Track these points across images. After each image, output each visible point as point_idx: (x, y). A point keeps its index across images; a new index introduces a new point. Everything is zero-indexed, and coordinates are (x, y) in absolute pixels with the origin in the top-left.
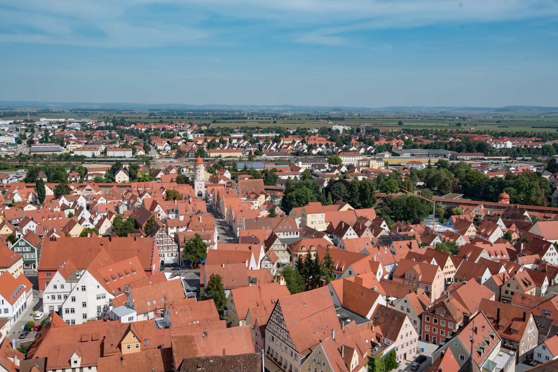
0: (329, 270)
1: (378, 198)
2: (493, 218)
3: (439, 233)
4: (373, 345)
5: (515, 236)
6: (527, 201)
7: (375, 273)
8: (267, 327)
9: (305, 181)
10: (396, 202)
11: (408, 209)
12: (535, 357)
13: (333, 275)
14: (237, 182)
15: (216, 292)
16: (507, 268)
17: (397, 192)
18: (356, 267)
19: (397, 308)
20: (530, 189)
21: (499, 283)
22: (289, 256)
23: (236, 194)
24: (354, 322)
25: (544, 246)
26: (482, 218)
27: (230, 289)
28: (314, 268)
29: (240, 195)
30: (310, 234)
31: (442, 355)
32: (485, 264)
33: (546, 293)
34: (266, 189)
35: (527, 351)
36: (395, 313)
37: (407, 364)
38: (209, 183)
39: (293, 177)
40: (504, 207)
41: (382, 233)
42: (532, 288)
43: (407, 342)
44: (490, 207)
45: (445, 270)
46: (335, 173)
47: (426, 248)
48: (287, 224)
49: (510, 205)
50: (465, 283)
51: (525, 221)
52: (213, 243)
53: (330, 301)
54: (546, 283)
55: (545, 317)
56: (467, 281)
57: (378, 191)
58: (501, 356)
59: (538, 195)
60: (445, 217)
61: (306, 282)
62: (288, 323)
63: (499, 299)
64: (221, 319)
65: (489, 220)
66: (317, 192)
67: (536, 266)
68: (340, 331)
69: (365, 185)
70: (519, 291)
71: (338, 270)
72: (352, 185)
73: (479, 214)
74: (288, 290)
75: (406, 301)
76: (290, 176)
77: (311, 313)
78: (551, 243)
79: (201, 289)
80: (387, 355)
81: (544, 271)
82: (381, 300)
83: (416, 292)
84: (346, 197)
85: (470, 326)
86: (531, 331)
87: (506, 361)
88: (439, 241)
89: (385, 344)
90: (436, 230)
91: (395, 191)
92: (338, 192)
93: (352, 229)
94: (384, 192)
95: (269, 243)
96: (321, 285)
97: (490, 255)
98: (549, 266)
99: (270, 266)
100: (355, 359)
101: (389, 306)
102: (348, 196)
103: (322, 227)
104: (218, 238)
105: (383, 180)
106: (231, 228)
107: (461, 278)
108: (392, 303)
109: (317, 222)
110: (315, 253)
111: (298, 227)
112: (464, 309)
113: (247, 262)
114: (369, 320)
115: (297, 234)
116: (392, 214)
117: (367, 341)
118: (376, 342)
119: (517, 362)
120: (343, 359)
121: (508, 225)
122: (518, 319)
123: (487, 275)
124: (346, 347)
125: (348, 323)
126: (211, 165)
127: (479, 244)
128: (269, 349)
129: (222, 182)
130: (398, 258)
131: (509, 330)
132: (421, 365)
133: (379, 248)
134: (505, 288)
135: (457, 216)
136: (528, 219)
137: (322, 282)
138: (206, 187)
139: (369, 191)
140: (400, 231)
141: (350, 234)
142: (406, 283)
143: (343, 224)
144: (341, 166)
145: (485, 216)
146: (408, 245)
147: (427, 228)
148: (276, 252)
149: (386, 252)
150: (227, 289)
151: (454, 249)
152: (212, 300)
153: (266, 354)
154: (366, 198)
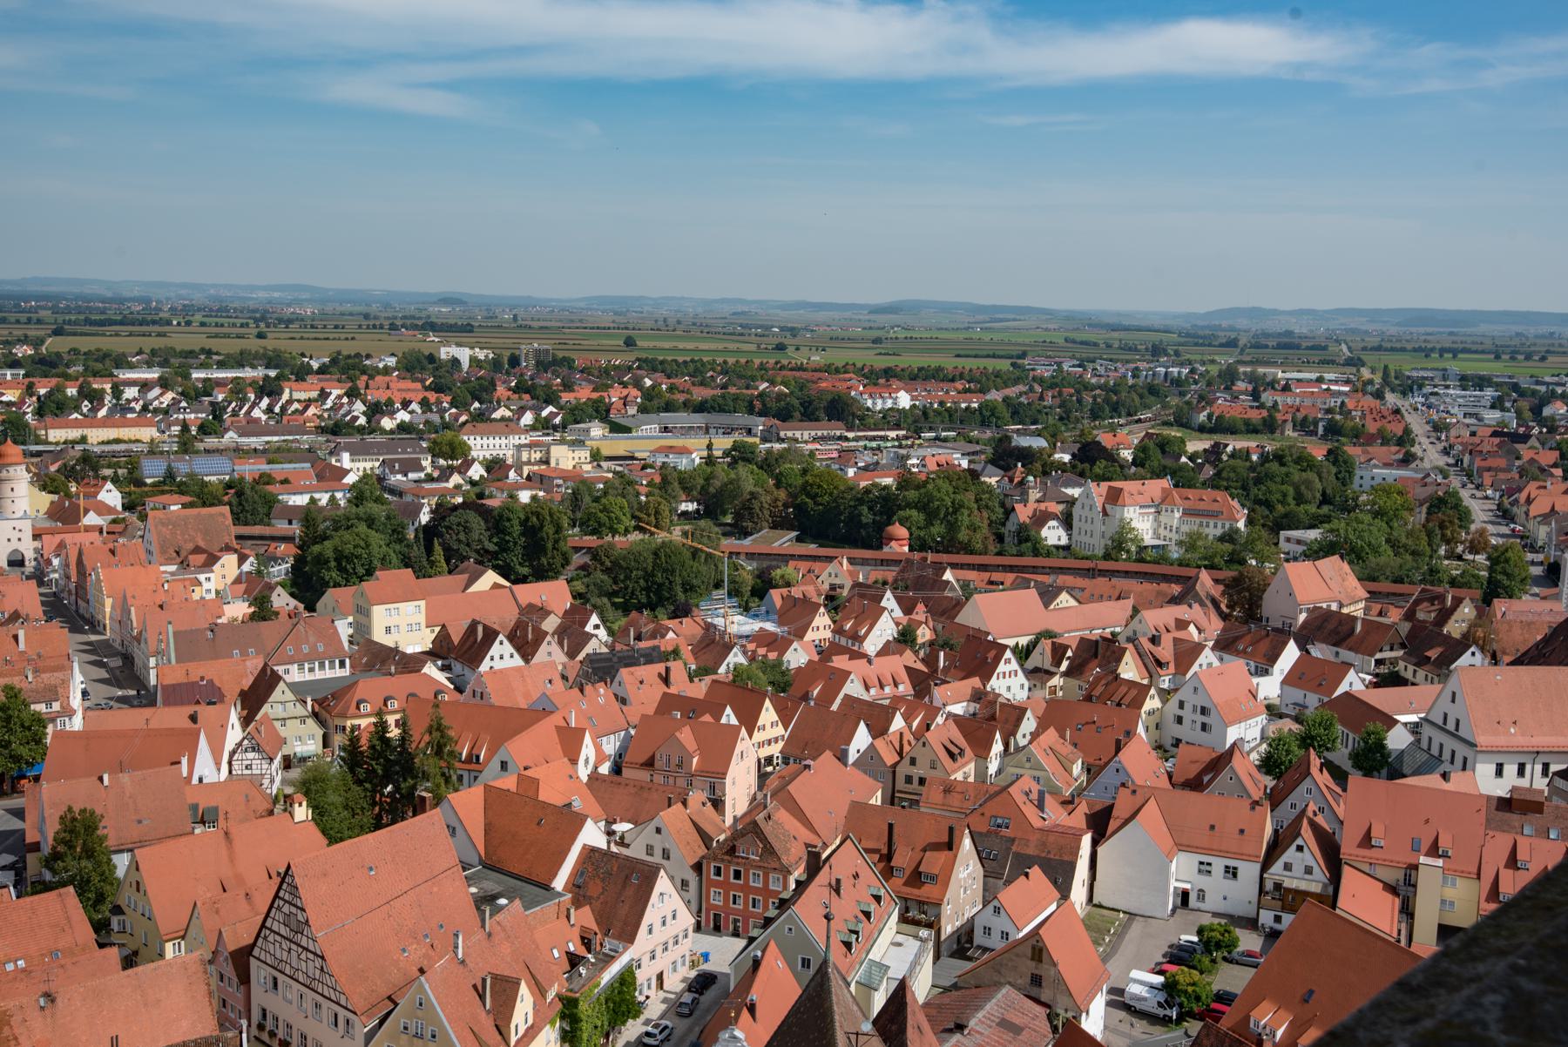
0: (443, 764)
1: (577, 549)
2: (872, 592)
3: (741, 637)
4: (574, 961)
5: (924, 634)
6: (950, 544)
7: (574, 761)
8: (256, 952)
9: (361, 510)
10: (624, 558)
11: (659, 578)
12: (979, 938)
13: (454, 778)
14: (143, 517)
15: (84, 863)
16: (908, 719)
17: (627, 531)
18: (520, 749)
19: (636, 851)
20: (955, 512)
21: (890, 758)
22: (319, 732)
23: (143, 555)
24: (517, 902)
25: (991, 655)
26: (845, 593)
27: (131, 850)
28: (396, 763)
29: (154, 558)
30: (383, 662)
31: (756, 964)
32: (858, 710)
33: (999, 772)
34: (239, 537)
35: (958, 924)
36: (632, 865)
37: (665, 1001)
38: (48, 524)
39: (324, 499)
40: (897, 562)
42: (967, 763)
43: (663, 940)
44: (864, 562)
45: (758, 736)
46: (451, 484)
47: (708, 679)
48: (312, 639)
49: (911, 556)
50: (807, 767)
51: (948, 593)
52: (70, 713)
53: (446, 853)
54: (998, 747)
55: (997, 833)
56: (814, 759)
57: (577, 530)
58: (900, 945)
59: (974, 528)
60: (753, 595)
61: (374, 804)
62: (321, 933)
63: (891, 799)
64: (101, 946)
65: (862, 596)
66: (400, 541)
67: (974, 707)
68: (479, 936)
69: (538, 515)
70: (938, 773)
71: (469, 760)
72: (501, 516)
73: (837, 581)
74: (320, 835)
75: (658, 831)
76: (317, 496)
77: (392, 893)
78: (1006, 647)
79: (32, 859)
80: (611, 985)
81: (993, 718)
82: (592, 835)
83: (685, 803)
84: (487, 551)
85: (823, 877)
86: (967, 870)
87: (911, 958)
88: (741, 660)
89: (606, 955)
90: (733, 629)
91: (621, 528)
92: (462, 536)
93: (506, 642)
94: (592, 533)
95: (254, 698)
96: (419, 807)
97: (867, 688)
98: (1002, 705)
99: (259, 766)
100: (524, 1008)
101: (614, 849)
102: (492, 547)
103: (417, 641)
104: (85, 693)
105: (587, 499)
106: (128, 659)
107: (798, 753)
108: (622, 838)
109: (404, 628)
110: (398, 716)
111: (346, 645)
112: (805, 835)
113: (185, 761)
114: (560, 895)
115: (342, 664)
116: (615, 594)
117: (555, 952)
118: (582, 951)
119: (937, 957)
120: (488, 1012)
121: (908, 609)
122: (936, 847)
123: (861, 739)
124: (495, 977)
125: (502, 908)
126: (53, 468)
127: (840, 662)
128: (264, 1016)
129: (92, 519)
130: (634, 712)
131: (916, 878)
132: (702, 999)
133: (582, 691)
134: (902, 771)
135: (784, 591)
136: (953, 589)
137: (423, 799)
138: (36, 537)
139: (551, 532)
140: (638, 638)
141: (502, 656)
142: (659, 779)
143: (480, 629)
144: (468, 464)
145: (853, 587)
146: (660, 675)
147: (709, 627)
148: (277, 724)
149: (601, 700)
150: (121, 851)
151: (778, 677)
152: (71, 889)
153: (254, 1031)
154: (543, 550)
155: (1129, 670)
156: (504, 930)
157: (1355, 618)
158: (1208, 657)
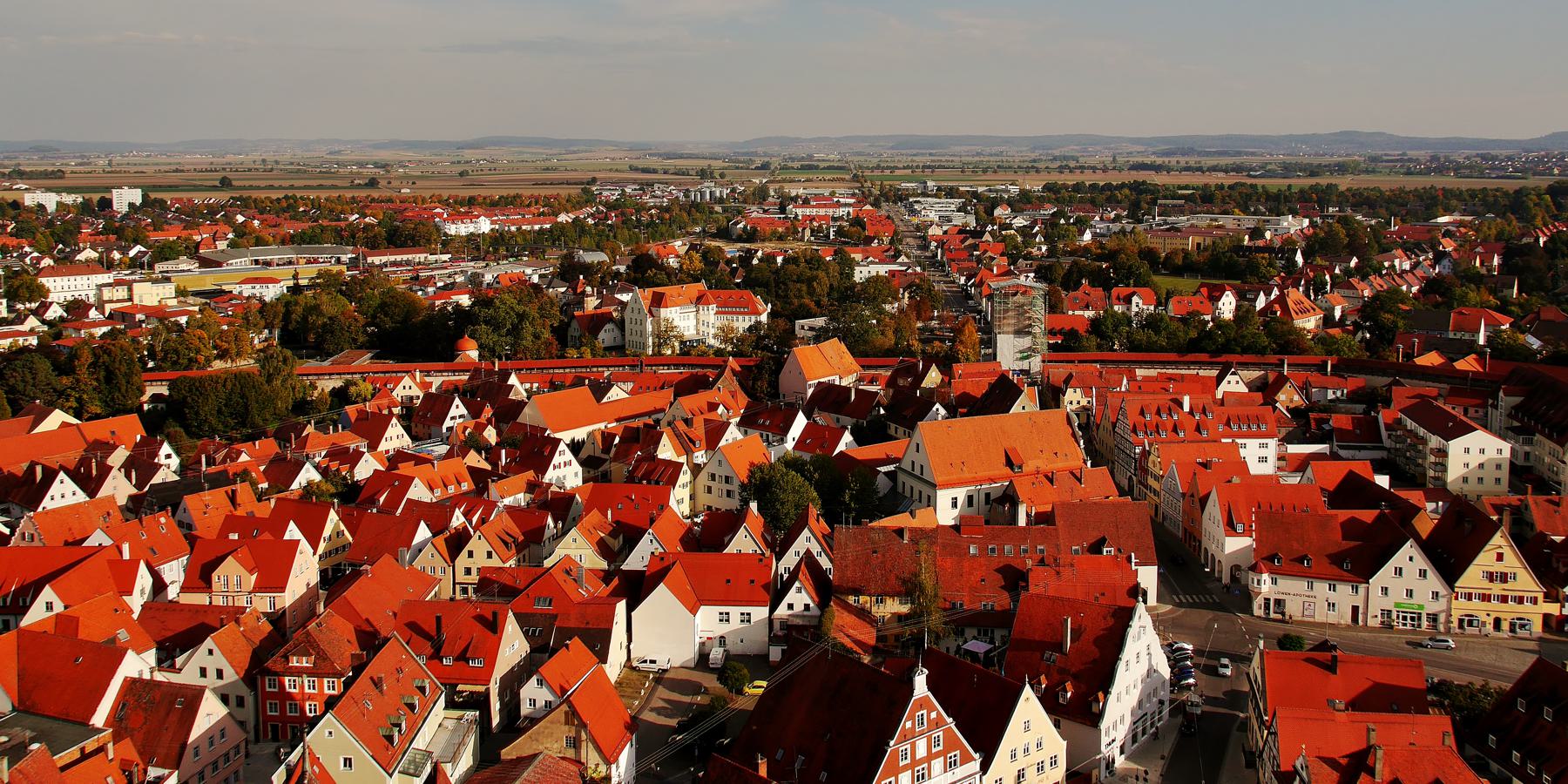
16: (468, 515)
32: (419, 511)
41: (157, 479)
51: (512, 396)
67: (529, 496)
78: (559, 441)
82: (138, 664)
83: (237, 621)
93: (67, 480)
97: (432, 489)
101: (160, 677)
114: (99, 731)
121: (475, 412)
127: (405, 469)
135: (360, 405)
136: (518, 393)
141: (64, 493)
143: (39, 469)
144: (46, 306)
155: (666, 451)
156: (26, 776)
157: (847, 390)
158: (733, 434)
